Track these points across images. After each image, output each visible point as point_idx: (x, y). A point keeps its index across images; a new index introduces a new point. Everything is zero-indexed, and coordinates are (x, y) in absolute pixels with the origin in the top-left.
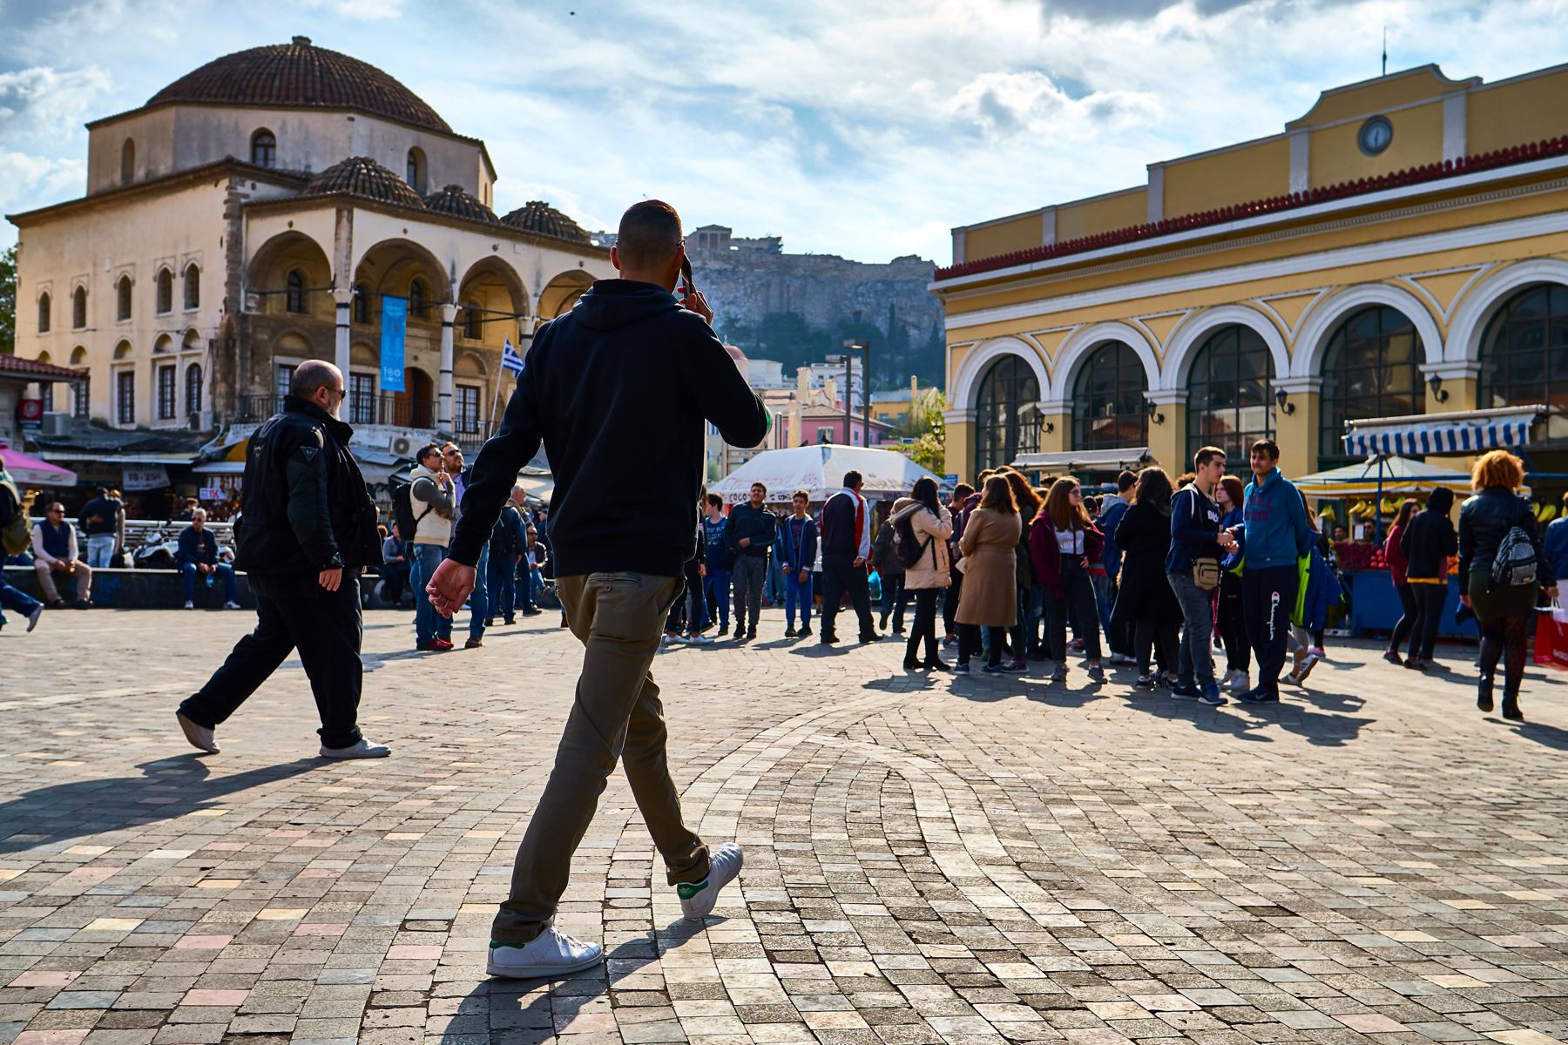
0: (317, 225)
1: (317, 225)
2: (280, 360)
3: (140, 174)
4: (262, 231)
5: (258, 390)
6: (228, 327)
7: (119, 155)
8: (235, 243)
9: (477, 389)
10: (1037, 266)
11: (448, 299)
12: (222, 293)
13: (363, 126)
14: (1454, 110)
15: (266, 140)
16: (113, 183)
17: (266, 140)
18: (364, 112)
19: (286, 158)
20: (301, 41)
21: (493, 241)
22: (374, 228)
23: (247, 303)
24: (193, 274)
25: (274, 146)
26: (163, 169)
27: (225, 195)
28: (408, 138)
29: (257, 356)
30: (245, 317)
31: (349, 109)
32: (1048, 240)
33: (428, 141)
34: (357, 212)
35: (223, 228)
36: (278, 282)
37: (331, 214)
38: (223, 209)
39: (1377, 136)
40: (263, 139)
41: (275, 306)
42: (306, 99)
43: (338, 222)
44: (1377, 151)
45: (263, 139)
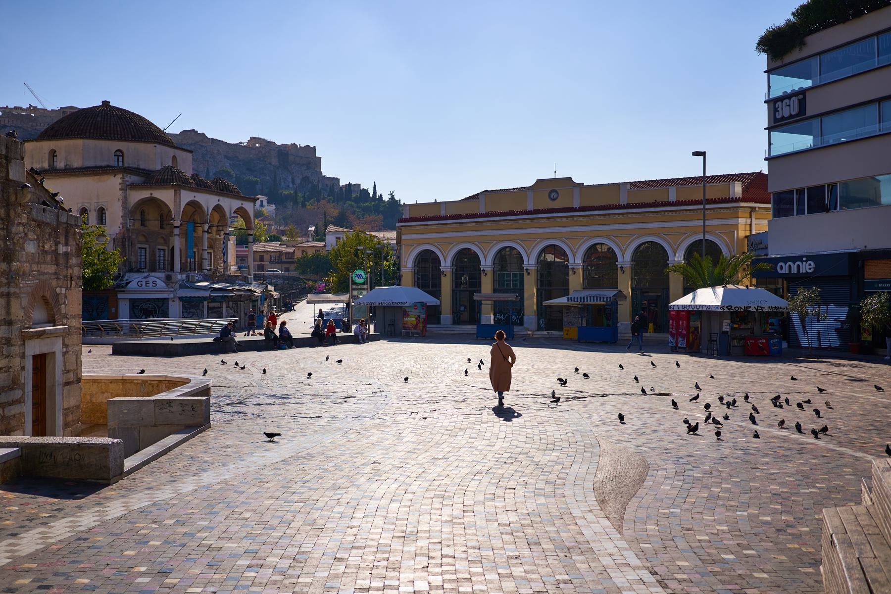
0: (166, 196)
1: (166, 196)
2: (140, 246)
3: (60, 164)
4: (138, 196)
5: (133, 259)
6: (124, 233)
7: (47, 155)
8: (125, 200)
9: (210, 253)
10: (441, 222)
11: (206, 222)
12: (121, 220)
13: (160, 148)
14: (576, 191)
15: (118, 153)
16: (42, 167)
17: (118, 153)
18: (159, 143)
19: (129, 162)
20: (106, 103)
21: (217, 198)
22: (187, 196)
23: (129, 223)
24: (101, 212)
25: (123, 156)
26: (76, 164)
27: (120, 181)
28: (171, 152)
29: (132, 244)
30: (128, 230)
31: (155, 142)
32: (443, 213)
33: (178, 153)
34: (182, 191)
35: (120, 194)
36: (138, 217)
37: (171, 192)
38: (120, 186)
39: (554, 195)
40: (119, 153)
41: (138, 224)
42: (133, 137)
43: (175, 195)
44: (554, 200)
45: (119, 153)
